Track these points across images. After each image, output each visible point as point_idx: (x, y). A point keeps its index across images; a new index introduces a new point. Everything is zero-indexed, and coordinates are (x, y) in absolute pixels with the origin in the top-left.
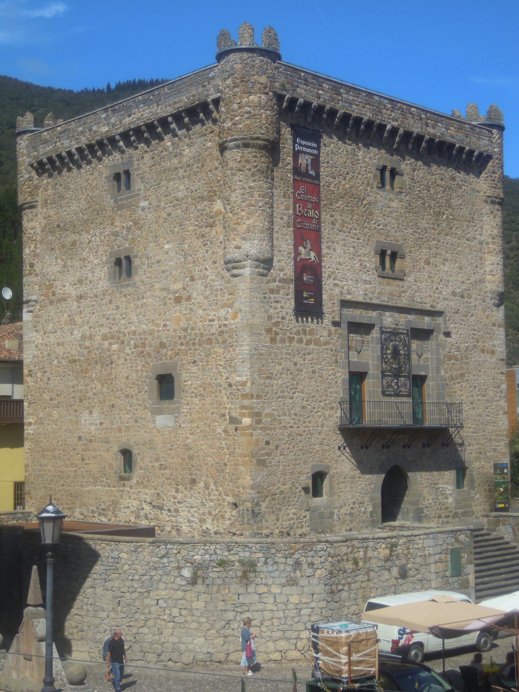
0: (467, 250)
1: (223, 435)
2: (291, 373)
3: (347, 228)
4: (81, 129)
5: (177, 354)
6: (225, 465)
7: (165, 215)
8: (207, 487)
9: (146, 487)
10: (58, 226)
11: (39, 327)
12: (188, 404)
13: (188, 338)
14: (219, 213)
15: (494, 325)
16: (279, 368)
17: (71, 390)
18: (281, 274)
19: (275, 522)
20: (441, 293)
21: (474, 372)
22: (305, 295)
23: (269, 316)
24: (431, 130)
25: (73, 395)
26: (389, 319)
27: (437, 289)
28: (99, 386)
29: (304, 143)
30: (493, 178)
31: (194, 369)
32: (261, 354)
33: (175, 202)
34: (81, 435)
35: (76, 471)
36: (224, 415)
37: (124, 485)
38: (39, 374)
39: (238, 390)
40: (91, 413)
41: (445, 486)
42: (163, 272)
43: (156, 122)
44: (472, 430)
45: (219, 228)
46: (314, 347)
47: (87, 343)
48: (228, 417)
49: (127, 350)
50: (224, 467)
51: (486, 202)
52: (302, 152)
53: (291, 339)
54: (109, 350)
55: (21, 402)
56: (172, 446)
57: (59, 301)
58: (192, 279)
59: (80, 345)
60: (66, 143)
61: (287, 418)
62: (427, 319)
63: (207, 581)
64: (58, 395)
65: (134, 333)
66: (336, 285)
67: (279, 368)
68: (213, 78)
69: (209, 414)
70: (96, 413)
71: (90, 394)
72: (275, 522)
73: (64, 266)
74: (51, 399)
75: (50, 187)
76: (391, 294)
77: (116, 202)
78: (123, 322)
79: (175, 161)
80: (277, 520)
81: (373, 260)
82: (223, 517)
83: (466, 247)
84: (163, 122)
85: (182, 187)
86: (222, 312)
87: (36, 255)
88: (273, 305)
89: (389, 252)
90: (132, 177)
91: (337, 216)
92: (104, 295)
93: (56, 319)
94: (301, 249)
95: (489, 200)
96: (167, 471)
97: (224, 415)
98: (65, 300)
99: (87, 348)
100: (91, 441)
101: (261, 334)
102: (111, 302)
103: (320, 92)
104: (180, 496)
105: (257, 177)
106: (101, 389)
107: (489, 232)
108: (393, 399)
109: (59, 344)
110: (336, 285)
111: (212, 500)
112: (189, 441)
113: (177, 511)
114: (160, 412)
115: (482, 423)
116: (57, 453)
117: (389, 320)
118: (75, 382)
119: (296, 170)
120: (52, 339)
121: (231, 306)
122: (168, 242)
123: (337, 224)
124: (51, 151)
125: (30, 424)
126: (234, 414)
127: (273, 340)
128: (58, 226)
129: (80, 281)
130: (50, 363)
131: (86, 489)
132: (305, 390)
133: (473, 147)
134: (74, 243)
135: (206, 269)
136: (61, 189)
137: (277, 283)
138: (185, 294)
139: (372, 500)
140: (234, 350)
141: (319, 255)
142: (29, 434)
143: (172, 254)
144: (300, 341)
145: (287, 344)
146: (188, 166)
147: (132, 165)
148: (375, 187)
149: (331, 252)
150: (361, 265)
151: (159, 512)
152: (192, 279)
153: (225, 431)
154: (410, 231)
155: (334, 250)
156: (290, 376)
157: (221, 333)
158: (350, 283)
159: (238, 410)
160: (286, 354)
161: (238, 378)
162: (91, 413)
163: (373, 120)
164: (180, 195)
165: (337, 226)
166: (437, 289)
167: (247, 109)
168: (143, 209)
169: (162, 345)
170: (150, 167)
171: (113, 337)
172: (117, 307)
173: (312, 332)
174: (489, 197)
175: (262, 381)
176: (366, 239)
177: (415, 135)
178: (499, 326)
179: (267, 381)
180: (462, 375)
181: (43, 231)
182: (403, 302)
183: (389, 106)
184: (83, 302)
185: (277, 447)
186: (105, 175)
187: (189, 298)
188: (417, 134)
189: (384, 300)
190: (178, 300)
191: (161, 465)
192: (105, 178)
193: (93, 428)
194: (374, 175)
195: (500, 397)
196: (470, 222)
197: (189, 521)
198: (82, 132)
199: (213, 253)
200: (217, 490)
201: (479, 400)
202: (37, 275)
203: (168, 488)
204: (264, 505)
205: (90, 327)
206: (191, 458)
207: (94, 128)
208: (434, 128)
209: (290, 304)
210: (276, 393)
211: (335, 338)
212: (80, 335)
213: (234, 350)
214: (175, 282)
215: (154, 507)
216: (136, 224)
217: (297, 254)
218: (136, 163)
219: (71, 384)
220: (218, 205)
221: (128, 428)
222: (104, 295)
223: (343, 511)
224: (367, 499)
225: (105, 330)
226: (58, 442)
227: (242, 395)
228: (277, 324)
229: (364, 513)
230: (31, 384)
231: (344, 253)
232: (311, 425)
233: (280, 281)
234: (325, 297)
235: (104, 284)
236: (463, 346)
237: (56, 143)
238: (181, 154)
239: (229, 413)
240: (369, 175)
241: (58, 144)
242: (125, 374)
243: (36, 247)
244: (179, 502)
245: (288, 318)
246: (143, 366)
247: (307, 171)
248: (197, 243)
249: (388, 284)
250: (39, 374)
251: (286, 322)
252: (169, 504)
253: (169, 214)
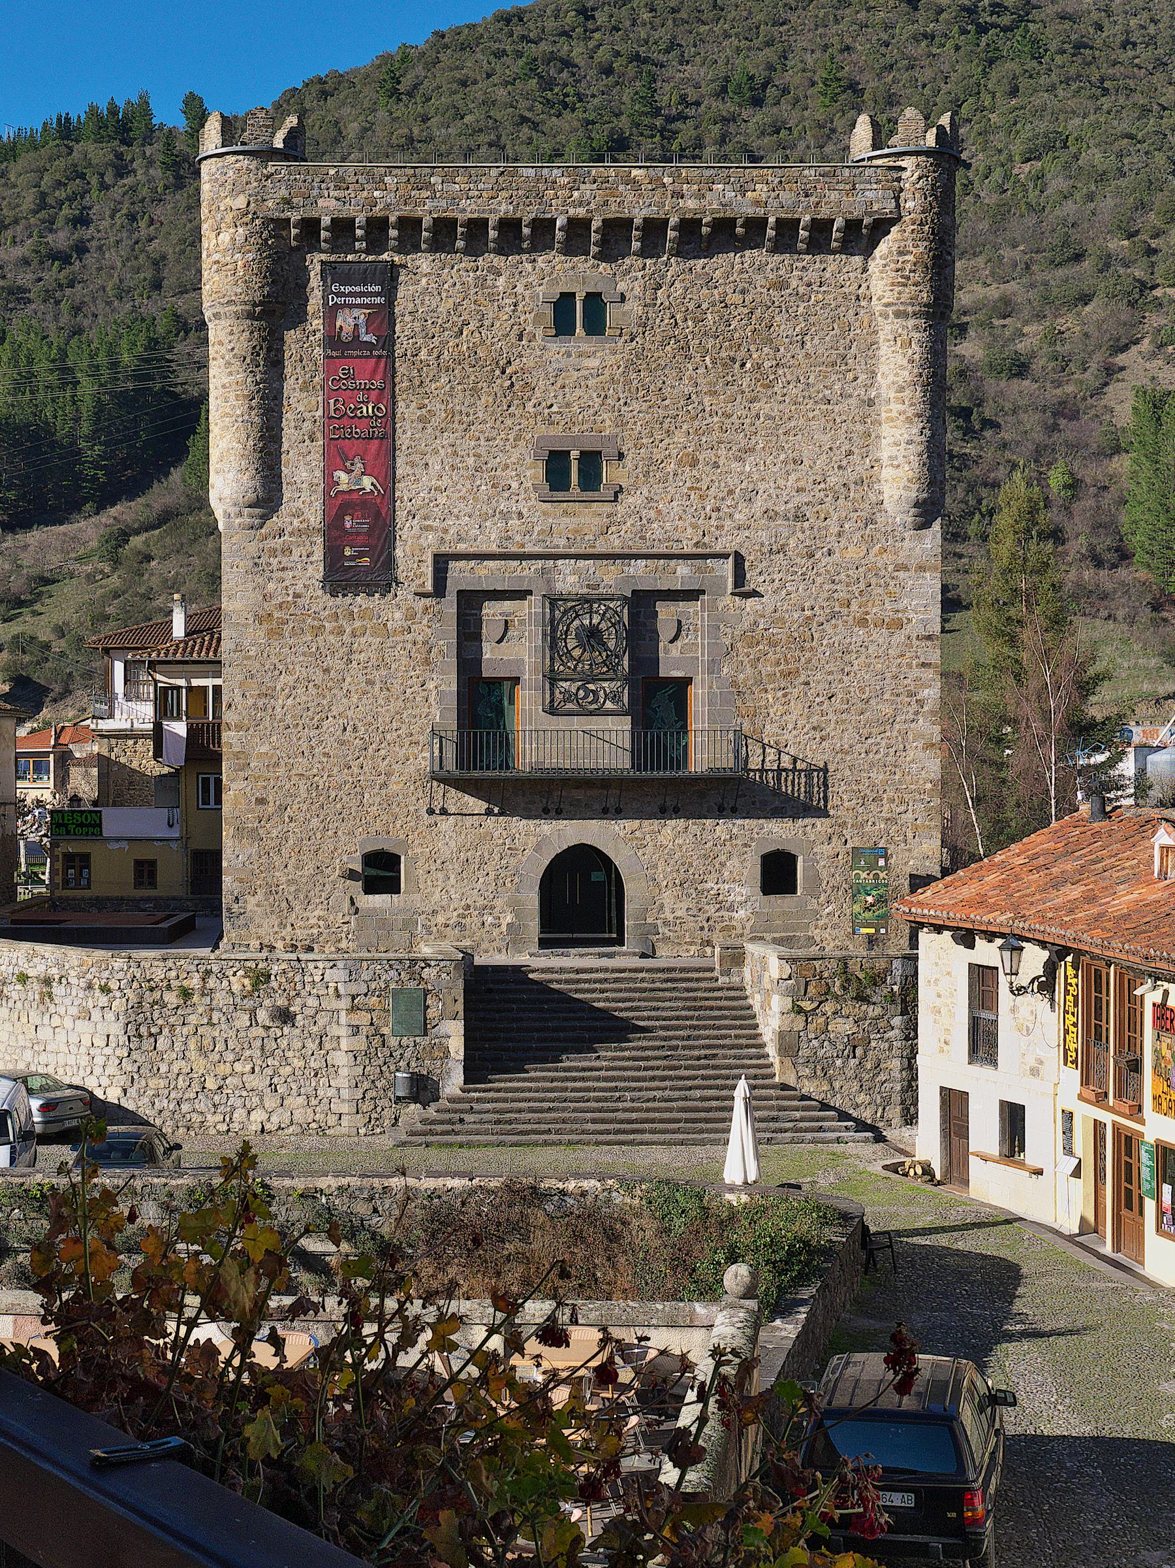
15: (906, 568)
18: (296, 522)
19: (276, 929)
21: (830, 667)
22: (348, 553)
24: (691, 204)
26: (572, 579)
29: (348, 289)
30: (899, 266)
52: (345, 305)
53: (318, 631)
62: (683, 569)
63: (11, 1004)
72: (276, 929)
89: (575, 454)
94: (342, 476)
95: (890, 310)
105: (233, 368)
107: (891, 378)
108: (577, 722)
110: (428, 528)
117: (569, 579)
119: (333, 341)
133: (824, 213)
141: (389, 479)
163: (518, 215)
165: (435, 421)
167: (216, 257)
174: (887, 305)
177: (638, 221)
178: (922, 568)
188: (645, 219)
189: (560, 544)
195: (917, 713)
204: (252, 901)
209: (316, 571)
211: (425, 622)
217: (330, 482)
247: (356, 336)
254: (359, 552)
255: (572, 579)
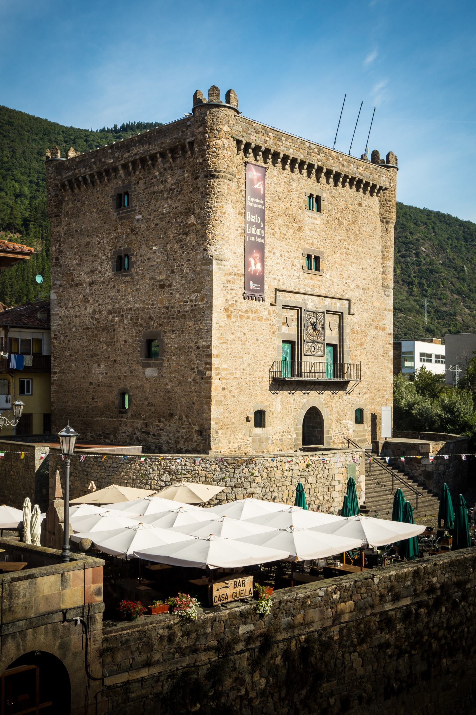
0: (368, 257)
1: (193, 383)
2: (242, 341)
3: (284, 238)
4: (93, 160)
5: (161, 325)
6: (194, 403)
7: (153, 226)
8: (180, 419)
9: (138, 418)
10: (76, 231)
11: (62, 304)
12: (168, 361)
13: (169, 313)
14: (193, 224)
15: (385, 310)
16: (233, 337)
17: (85, 349)
20: (349, 286)
23: (226, 300)
24: (345, 169)
25: (86, 352)
26: (312, 304)
27: (346, 283)
28: (105, 347)
31: (173, 336)
32: (220, 326)
33: (161, 216)
34: (91, 381)
35: (88, 407)
36: (193, 369)
37: (122, 417)
38: (62, 338)
39: (204, 351)
40: (99, 366)
41: (347, 421)
42: (152, 266)
43: (147, 157)
44: (367, 383)
45: (192, 236)
46: (258, 322)
47: (97, 316)
48: (196, 370)
49: (125, 322)
50: (193, 405)
51: (382, 222)
53: (241, 317)
54: (112, 321)
55: (49, 357)
56: (156, 390)
57: (77, 285)
58: (173, 272)
59: (92, 317)
60: (82, 170)
61: (238, 372)
64: (75, 353)
65: (130, 309)
66: (275, 279)
67: (233, 337)
68: (190, 126)
69: (183, 368)
70: (103, 366)
71: (99, 353)
73: (81, 260)
74: (71, 355)
75: (70, 203)
76: (313, 286)
77: (118, 214)
78: (123, 301)
79: (161, 186)
80: (230, 443)
81: (301, 261)
82: (191, 440)
83: (367, 254)
84: (153, 158)
85: (166, 206)
86: (194, 296)
87: (61, 252)
88: (230, 292)
89: (313, 257)
90: (130, 197)
91: (277, 229)
92: (109, 281)
93: (74, 298)
95: (384, 220)
96: (153, 408)
97: (193, 369)
98: (81, 285)
99: (96, 319)
100: (99, 386)
101: (221, 312)
102: (114, 287)
103: (268, 139)
104: (161, 425)
106: (106, 349)
109: (76, 316)
111: (184, 428)
112: (168, 387)
113: (159, 435)
114: (149, 366)
115: (375, 378)
116: (75, 394)
118: (88, 344)
120: (72, 312)
121: (200, 292)
122: (156, 245)
123: (276, 235)
124: (71, 176)
125: (55, 373)
126: (201, 369)
127: (229, 316)
128: (76, 231)
129: (92, 271)
130: (71, 330)
131: (95, 419)
132: (251, 353)
134: (88, 244)
135: (182, 265)
136: (79, 204)
137: (233, 276)
138: (167, 283)
139: (296, 430)
140: (201, 323)
142: (54, 380)
143: (159, 254)
144: (248, 318)
145: (239, 319)
146: (171, 189)
147: (131, 188)
148: (304, 208)
149: (272, 254)
150: (293, 265)
151: (146, 436)
152: (173, 272)
153: (194, 380)
154: (328, 241)
155: (274, 253)
156: (240, 342)
157: (192, 310)
158: (285, 277)
159: (204, 365)
160: (238, 326)
161: (203, 343)
162: (99, 366)
164: (165, 211)
166: (346, 283)
168: (138, 220)
169: (151, 318)
170: (143, 190)
171: (115, 312)
172: (119, 291)
173: (256, 311)
174: (384, 218)
175: (220, 346)
176: (297, 246)
178: (389, 310)
179: (224, 346)
180: (361, 345)
181: (65, 234)
182: (322, 292)
183: (316, 150)
184: (95, 287)
185: (230, 392)
186: (110, 195)
187: (170, 286)
189: (309, 290)
190: (162, 287)
191: (149, 403)
192: (111, 197)
193: (100, 376)
194: (304, 200)
196: (370, 236)
197: (168, 442)
198: (94, 163)
199: (188, 253)
200: (188, 421)
201: (373, 362)
202: (61, 266)
203: (154, 419)
205: (99, 305)
206: (170, 398)
207: (103, 160)
208: (348, 168)
210: (230, 354)
212: (91, 311)
213: (201, 323)
214: (160, 273)
215: (143, 432)
216: (132, 231)
218: (133, 187)
219: (85, 345)
220: (192, 219)
221: (125, 376)
222: (109, 281)
223: (275, 437)
224: (292, 430)
225: (110, 307)
226: (75, 386)
227: (206, 355)
228: (232, 305)
229: (290, 439)
230: (56, 344)
231: (281, 255)
232: (255, 376)
233: (235, 275)
234: (266, 287)
235: (109, 274)
236: (363, 324)
237: (75, 170)
238: (166, 181)
239: (197, 367)
240: (300, 200)
241: (77, 170)
242: (124, 339)
243: (60, 246)
244: (161, 430)
245: (239, 300)
246: (137, 333)
248: (177, 246)
249: (312, 279)
250: (62, 338)
251: (238, 304)
252: (153, 430)
253: (157, 225)
254: (254, 286)
255: (312, 304)
